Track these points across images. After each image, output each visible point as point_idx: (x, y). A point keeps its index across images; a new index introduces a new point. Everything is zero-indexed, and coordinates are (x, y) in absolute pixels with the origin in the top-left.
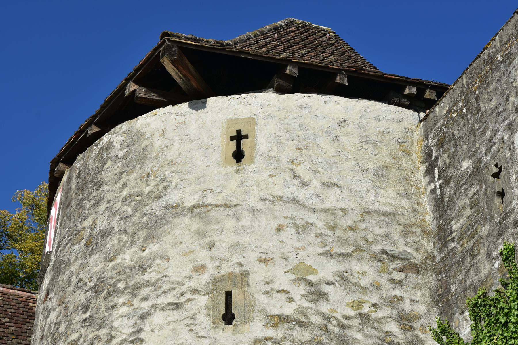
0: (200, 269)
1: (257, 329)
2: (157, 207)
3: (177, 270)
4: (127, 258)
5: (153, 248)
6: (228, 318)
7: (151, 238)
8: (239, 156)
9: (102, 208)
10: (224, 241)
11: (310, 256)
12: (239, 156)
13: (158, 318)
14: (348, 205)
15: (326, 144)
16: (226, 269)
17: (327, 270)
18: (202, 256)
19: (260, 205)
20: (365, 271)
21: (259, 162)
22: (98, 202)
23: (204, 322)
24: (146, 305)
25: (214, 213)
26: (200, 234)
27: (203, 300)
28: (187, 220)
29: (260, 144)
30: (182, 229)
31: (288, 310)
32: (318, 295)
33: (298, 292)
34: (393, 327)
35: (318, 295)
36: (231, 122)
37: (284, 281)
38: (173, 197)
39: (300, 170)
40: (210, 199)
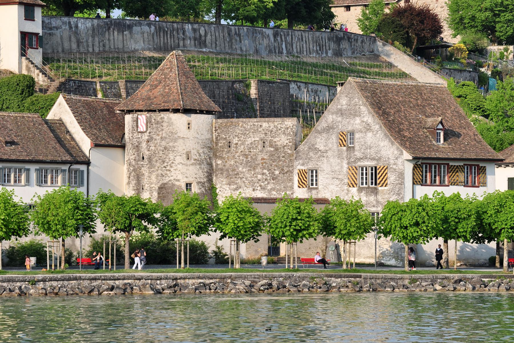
0: (184, 149)
1: (193, 161)
2: (176, 136)
3: (180, 149)
4: (171, 144)
5: (176, 144)
6: (188, 159)
7: (175, 142)
8: (189, 128)
9: (164, 132)
10: (188, 145)
11: (199, 148)
12: (189, 128)
13: (178, 157)
14: (204, 138)
15: (201, 125)
16: (188, 150)
17: (201, 151)
18: (184, 147)
19: (193, 139)
20: (206, 150)
21: (192, 129)
22: (163, 130)
23: (185, 159)
24: (175, 155)
25: (186, 140)
26: (184, 143)
27: (185, 155)
28: (181, 140)
29: (193, 126)
30: (181, 141)
31: (196, 158)
32: (200, 155)
33: (197, 155)
34: (208, 160)
35: (200, 155)
36: (188, 120)
37: (196, 153)
38: (179, 135)
39: (198, 131)
40: (185, 137)
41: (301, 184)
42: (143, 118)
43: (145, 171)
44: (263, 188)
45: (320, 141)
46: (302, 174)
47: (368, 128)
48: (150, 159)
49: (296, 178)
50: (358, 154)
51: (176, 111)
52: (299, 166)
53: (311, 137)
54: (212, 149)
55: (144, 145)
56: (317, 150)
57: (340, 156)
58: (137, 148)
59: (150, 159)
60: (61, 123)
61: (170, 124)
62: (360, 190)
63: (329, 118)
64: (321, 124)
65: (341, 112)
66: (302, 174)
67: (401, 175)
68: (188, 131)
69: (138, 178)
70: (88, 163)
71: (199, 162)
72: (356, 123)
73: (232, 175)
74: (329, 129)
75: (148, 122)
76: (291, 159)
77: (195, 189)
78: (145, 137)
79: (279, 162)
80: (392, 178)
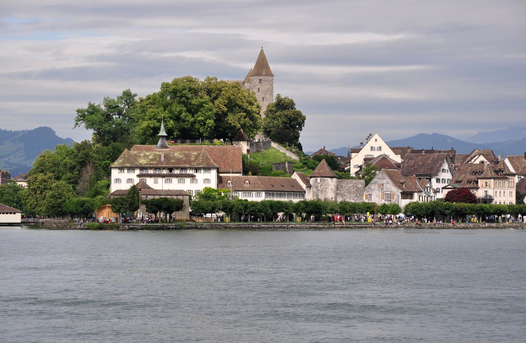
41: (366, 198)
42: (319, 179)
43: (320, 194)
44: (353, 199)
45: (372, 186)
46: (366, 195)
47: (388, 183)
48: (321, 191)
49: (364, 197)
50: (385, 190)
51: (329, 177)
52: (365, 193)
53: (369, 185)
54: (337, 188)
55: (319, 187)
56: (371, 189)
57: (379, 190)
58: (317, 187)
59: (321, 191)
60: (295, 180)
61: (327, 181)
62: (385, 200)
63: (375, 180)
64: (373, 181)
65: (379, 178)
66: (366, 195)
67: (399, 196)
68: (332, 183)
69: (317, 196)
70: (305, 192)
71: (334, 192)
72: (384, 181)
73: (342, 195)
74: (375, 183)
75: (321, 180)
76: (363, 192)
77: (333, 199)
78: (320, 184)
79: (359, 192)
80: (396, 197)
